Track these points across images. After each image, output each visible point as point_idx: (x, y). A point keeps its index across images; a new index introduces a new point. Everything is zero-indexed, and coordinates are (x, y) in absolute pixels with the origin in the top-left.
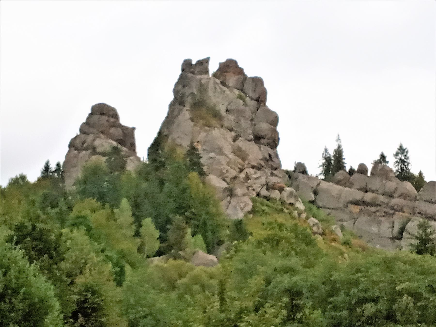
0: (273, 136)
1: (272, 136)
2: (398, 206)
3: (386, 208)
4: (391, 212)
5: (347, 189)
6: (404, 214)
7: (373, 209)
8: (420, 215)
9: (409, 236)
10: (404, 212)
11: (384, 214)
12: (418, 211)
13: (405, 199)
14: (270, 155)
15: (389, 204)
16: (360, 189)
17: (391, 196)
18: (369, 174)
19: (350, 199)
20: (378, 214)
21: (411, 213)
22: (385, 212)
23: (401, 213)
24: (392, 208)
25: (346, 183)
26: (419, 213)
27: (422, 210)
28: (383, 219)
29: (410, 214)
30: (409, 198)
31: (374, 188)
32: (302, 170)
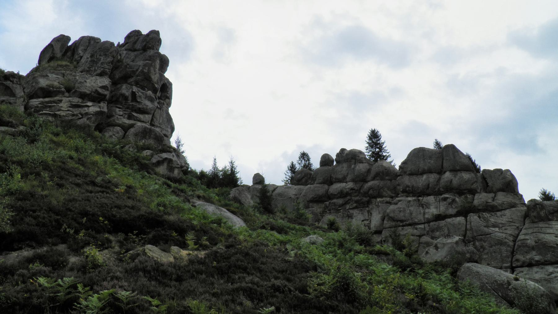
0: (146, 71)
1: (142, 71)
2: (373, 191)
3: (357, 196)
4: (365, 199)
5: (309, 186)
6: (384, 199)
7: (340, 201)
8: (405, 194)
9: (393, 224)
10: (382, 197)
11: (355, 205)
12: (401, 188)
13: (382, 179)
14: (133, 94)
15: (362, 191)
16: (323, 183)
17: (365, 181)
18: (335, 163)
19: (310, 196)
20: (348, 207)
21: (393, 195)
22: (356, 202)
23: (378, 200)
24: (366, 194)
25: (306, 181)
26: (404, 191)
27: (408, 186)
28: (355, 212)
29: (392, 197)
30: (387, 178)
31: (340, 177)
32: (258, 181)
